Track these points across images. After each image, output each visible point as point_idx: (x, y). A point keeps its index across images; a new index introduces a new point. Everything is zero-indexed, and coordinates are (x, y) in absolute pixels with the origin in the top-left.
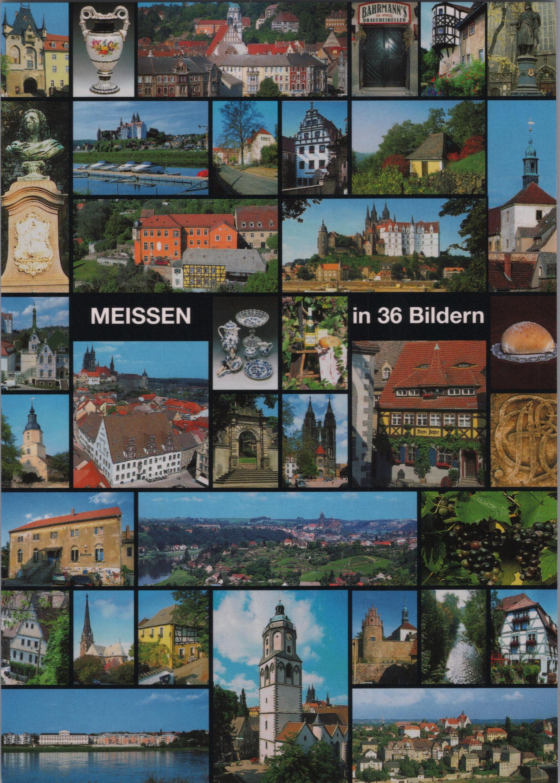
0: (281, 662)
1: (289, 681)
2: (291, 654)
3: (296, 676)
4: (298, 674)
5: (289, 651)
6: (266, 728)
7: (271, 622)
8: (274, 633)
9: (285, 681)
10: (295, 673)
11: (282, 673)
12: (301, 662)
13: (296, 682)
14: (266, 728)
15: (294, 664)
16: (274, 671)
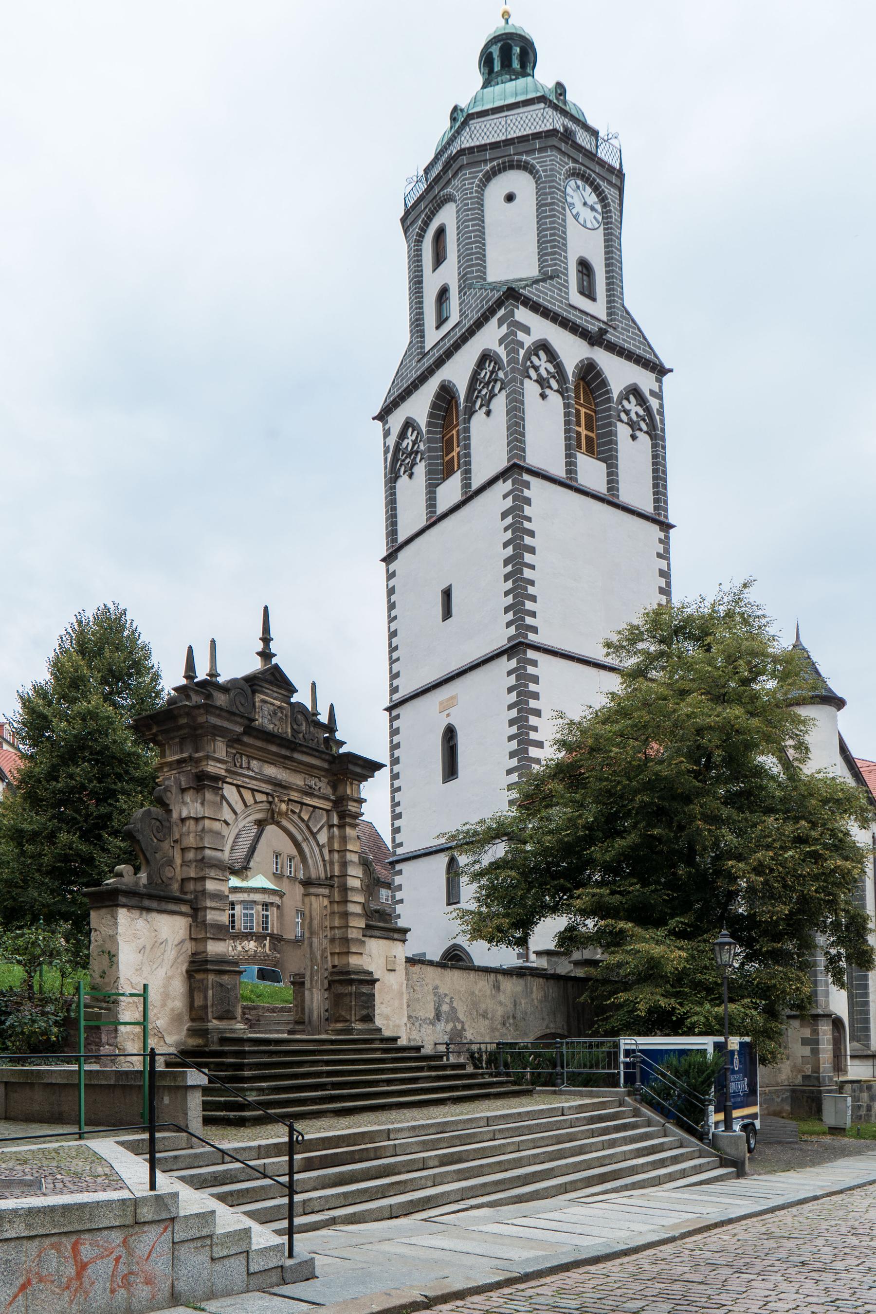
0: (544, 346)
1: (591, 473)
2: (598, 309)
3: (633, 452)
4: (644, 440)
5: (588, 292)
6: (451, 770)
7: (462, 120)
8: (488, 177)
9: (571, 466)
10: (623, 431)
11: (546, 422)
12: (660, 371)
13: (636, 490)
14: (451, 770)
15: (619, 374)
16: (500, 404)
